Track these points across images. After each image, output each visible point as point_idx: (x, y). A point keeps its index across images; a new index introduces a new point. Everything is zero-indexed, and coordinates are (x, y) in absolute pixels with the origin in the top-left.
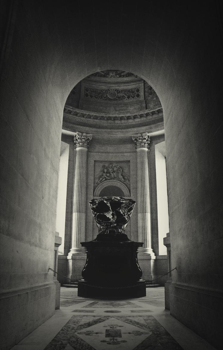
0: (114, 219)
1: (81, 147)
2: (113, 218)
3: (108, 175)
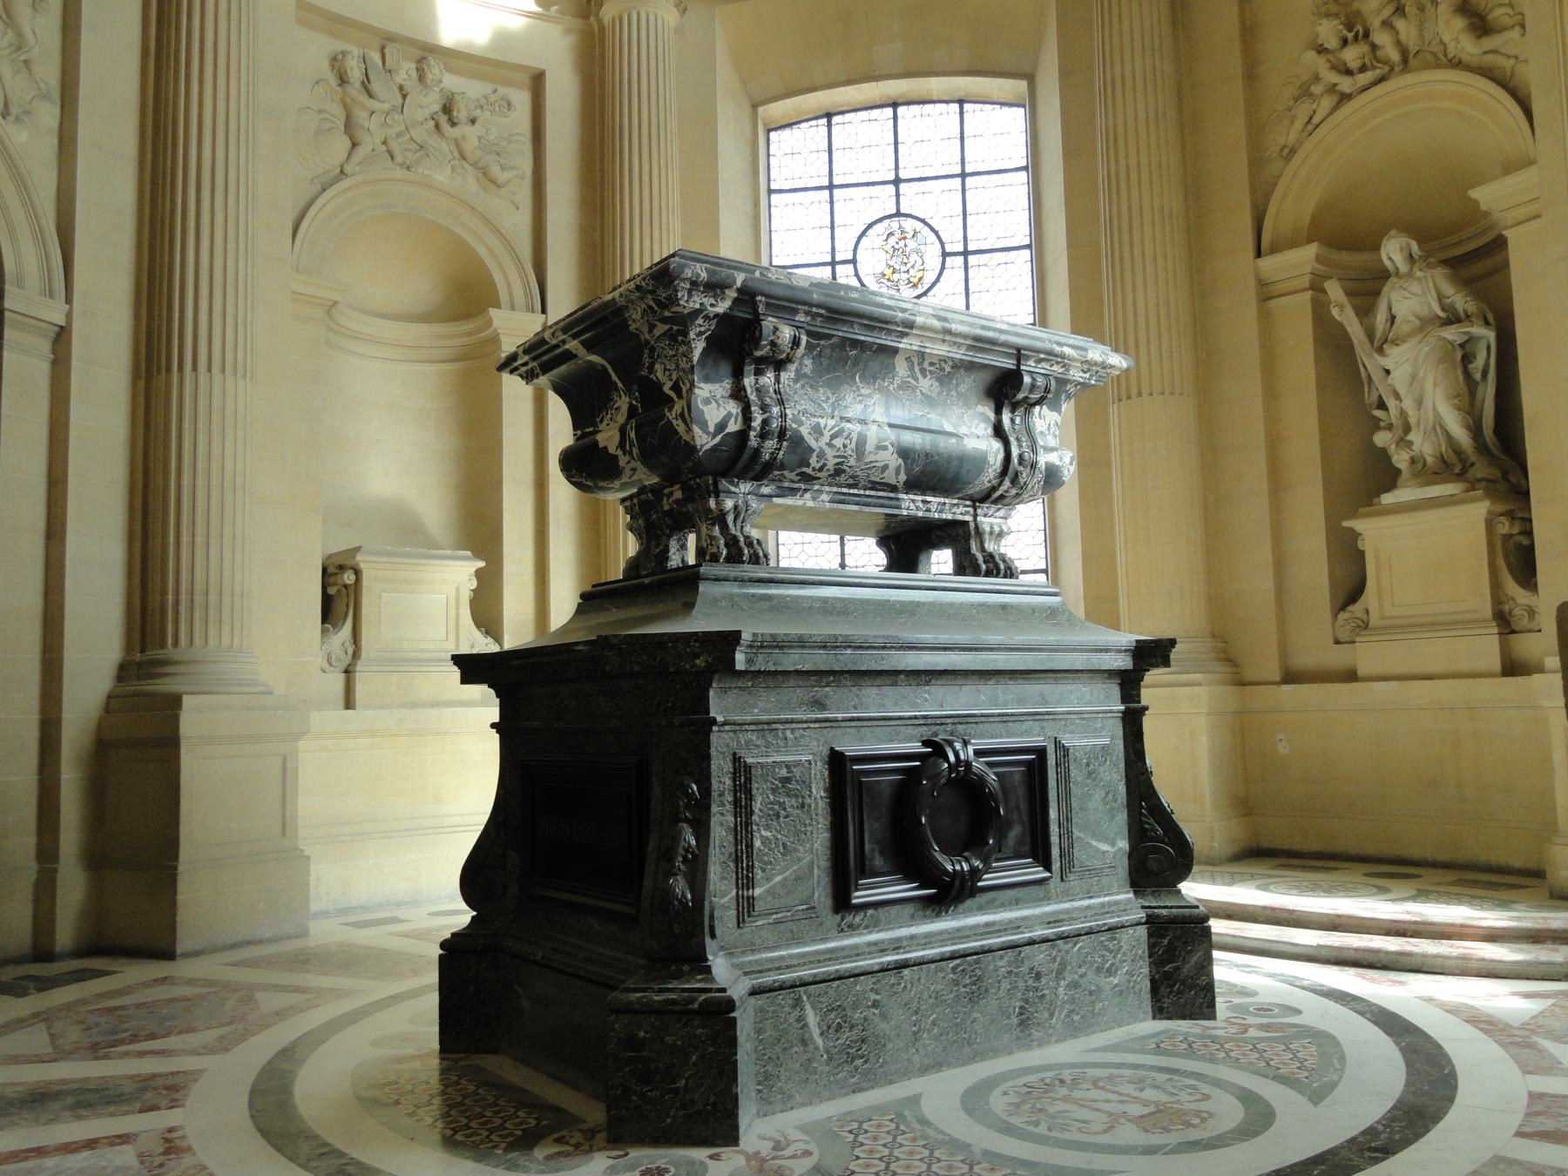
0: (631, 453)
2: (622, 445)
3: (1351, 56)
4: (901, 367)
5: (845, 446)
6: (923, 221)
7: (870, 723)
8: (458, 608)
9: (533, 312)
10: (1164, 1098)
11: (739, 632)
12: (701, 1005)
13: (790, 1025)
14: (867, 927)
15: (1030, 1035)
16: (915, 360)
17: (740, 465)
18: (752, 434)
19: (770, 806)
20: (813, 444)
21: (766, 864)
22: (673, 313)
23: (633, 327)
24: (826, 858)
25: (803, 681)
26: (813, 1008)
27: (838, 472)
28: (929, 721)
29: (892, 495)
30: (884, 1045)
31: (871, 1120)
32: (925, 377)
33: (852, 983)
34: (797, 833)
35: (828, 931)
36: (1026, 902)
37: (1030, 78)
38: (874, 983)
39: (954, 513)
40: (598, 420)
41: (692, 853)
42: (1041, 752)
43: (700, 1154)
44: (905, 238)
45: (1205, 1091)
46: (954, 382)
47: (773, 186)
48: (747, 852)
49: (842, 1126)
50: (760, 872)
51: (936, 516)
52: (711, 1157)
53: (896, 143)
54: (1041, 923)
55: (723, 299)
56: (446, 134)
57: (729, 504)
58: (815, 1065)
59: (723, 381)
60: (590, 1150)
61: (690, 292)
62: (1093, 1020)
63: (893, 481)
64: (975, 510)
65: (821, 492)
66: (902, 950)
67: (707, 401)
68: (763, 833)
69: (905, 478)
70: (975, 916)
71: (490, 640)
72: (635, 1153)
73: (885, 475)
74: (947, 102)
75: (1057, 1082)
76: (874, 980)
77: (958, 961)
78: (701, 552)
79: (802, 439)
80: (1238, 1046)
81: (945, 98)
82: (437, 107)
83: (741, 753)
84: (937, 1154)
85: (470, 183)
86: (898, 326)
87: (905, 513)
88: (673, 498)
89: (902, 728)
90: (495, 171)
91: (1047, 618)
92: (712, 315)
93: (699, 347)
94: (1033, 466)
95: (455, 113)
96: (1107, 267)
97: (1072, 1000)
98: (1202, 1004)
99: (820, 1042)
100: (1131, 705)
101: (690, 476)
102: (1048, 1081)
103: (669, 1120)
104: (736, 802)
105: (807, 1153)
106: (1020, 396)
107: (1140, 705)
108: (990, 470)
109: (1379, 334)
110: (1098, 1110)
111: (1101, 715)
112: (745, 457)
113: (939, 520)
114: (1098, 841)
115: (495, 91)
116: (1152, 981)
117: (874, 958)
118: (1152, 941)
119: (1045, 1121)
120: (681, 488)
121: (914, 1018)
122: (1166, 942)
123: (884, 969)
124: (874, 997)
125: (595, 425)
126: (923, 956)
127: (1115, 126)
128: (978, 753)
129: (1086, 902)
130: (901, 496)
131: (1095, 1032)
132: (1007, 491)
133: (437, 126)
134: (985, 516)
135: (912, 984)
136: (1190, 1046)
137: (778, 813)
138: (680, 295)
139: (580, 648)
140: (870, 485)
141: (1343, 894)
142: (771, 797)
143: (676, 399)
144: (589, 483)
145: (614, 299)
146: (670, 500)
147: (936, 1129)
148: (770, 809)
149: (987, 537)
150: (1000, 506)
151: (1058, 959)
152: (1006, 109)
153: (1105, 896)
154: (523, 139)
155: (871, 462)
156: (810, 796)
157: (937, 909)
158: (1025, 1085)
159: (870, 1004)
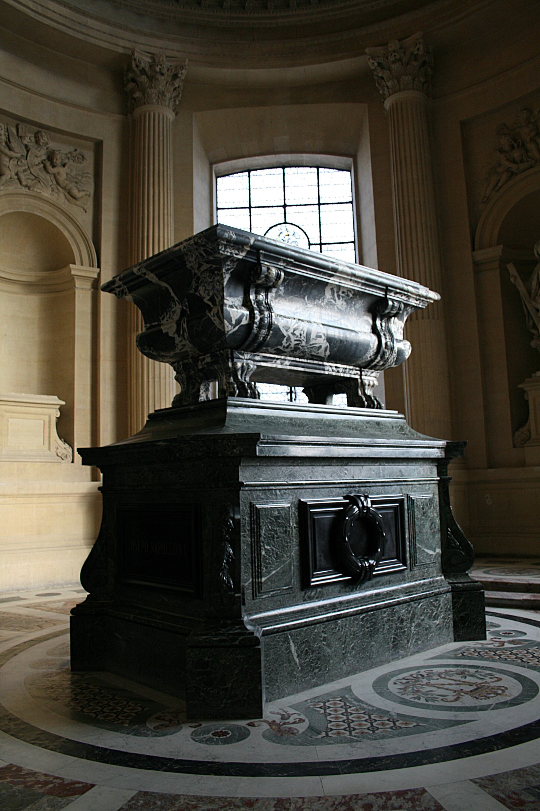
0: (183, 336)
1: (393, 94)
2: (178, 331)
3: (516, 154)
4: (328, 294)
5: (301, 335)
6: (298, 227)
7: (318, 486)
8: (50, 428)
9: (93, 267)
10: (479, 681)
11: (259, 434)
12: (240, 642)
13: (283, 651)
14: (317, 598)
15: (398, 652)
16: (335, 290)
17: (247, 343)
18: (255, 325)
19: (269, 532)
20: (285, 333)
21: (267, 564)
22: (214, 257)
23: (189, 266)
24: (297, 560)
25: (285, 462)
26: (293, 642)
27: (296, 348)
28: (348, 485)
29: (321, 363)
30: (329, 661)
31: (329, 701)
32: (339, 299)
33: (313, 628)
34: (283, 547)
35: (298, 600)
36: (393, 582)
37: (354, 157)
38: (324, 628)
39: (351, 374)
40: (161, 318)
41: (232, 558)
42: (401, 502)
43: (243, 723)
44: (289, 235)
45: (496, 676)
46: (353, 303)
47: (219, 207)
48: (258, 558)
49: (315, 705)
50: (264, 568)
51: (342, 375)
52: (249, 725)
53: (284, 187)
54: (403, 594)
55: (242, 251)
56: (50, 171)
57: (239, 365)
58: (295, 673)
59: (238, 297)
60: (179, 723)
61: (225, 248)
62: (427, 643)
63: (322, 355)
64: (361, 371)
65: (285, 360)
66: (336, 610)
67: (231, 307)
68: (266, 547)
69: (329, 353)
70: (370, 590)
71: (67, 446)
72: (204, 725)
73: (320, 351)
74: (311, 167)
75: (420, 676)
76: (323, 626)
77: (364, 615)
78: (222, 391)
79: (279, 329)
80: (503, 652)
81: (310, 165)
82: (44, 157)
83: (254, 502)
84: (372, 717)
85: (61, 199)
86: (329, 270)
87: (327, 373)
88: (205, 361)
89: (334, 489)
90: (75, 192)
91: (399, 430)
92: (235, 260)
93: (227, 277)
94: (392, 349)
95: (55, 160)
96: (399, 253)
97: (418, 633)
98: (479, 632)
99: (297, 660)
100: (443, 477)
101: (217, 349)
102: (414, 676)
103: (222, 706)
104: (252, 530)
105: (302, 721)
106: (387, 311)
107: (448, 477)
108: (371, 351)
109: (533, 291)
110: (447, 689)
111: (428, 482)
112: (250, 338)
113: (344, 377)
114: (428, 549)
115: (76, 150)
116: (454, 622)
117: (323, 614)
118: (454, 600)
119: (423, 697)
120: (210, 356)
121: (343, 646)
122: (461, 601)
123: (329, 620)
124: (324, 635)
125: (159, 321)
126: (348, 613)
127: (402, 182)
128: (373, 503)
129: (422, 581)
130: (325, 363)
131: (428, 649)
132: (378, 362)
133: (45, 167)
134: (366, 375)
135: (342, 628)
136: (479, 653)
137: (274, 536)
138: (220, 247)
139: (160, 443)
140: (310, 357)
141: (527, 574)
142: (270, 527)
143: (212, 306)
144: (154, 353)
145: (180, 249)
146: (203, 363)
147: (367, 704)
148: (269, 534)
149: (367, 387)
150: (373, 371)
151: (411, 612)
152: (341, 172)
153: (431, 578)
154: (90, 175)
155: (313, 344)
156: (289, 526)
157: (352, 588)
158: (403, 679)
159: (322, 639)
